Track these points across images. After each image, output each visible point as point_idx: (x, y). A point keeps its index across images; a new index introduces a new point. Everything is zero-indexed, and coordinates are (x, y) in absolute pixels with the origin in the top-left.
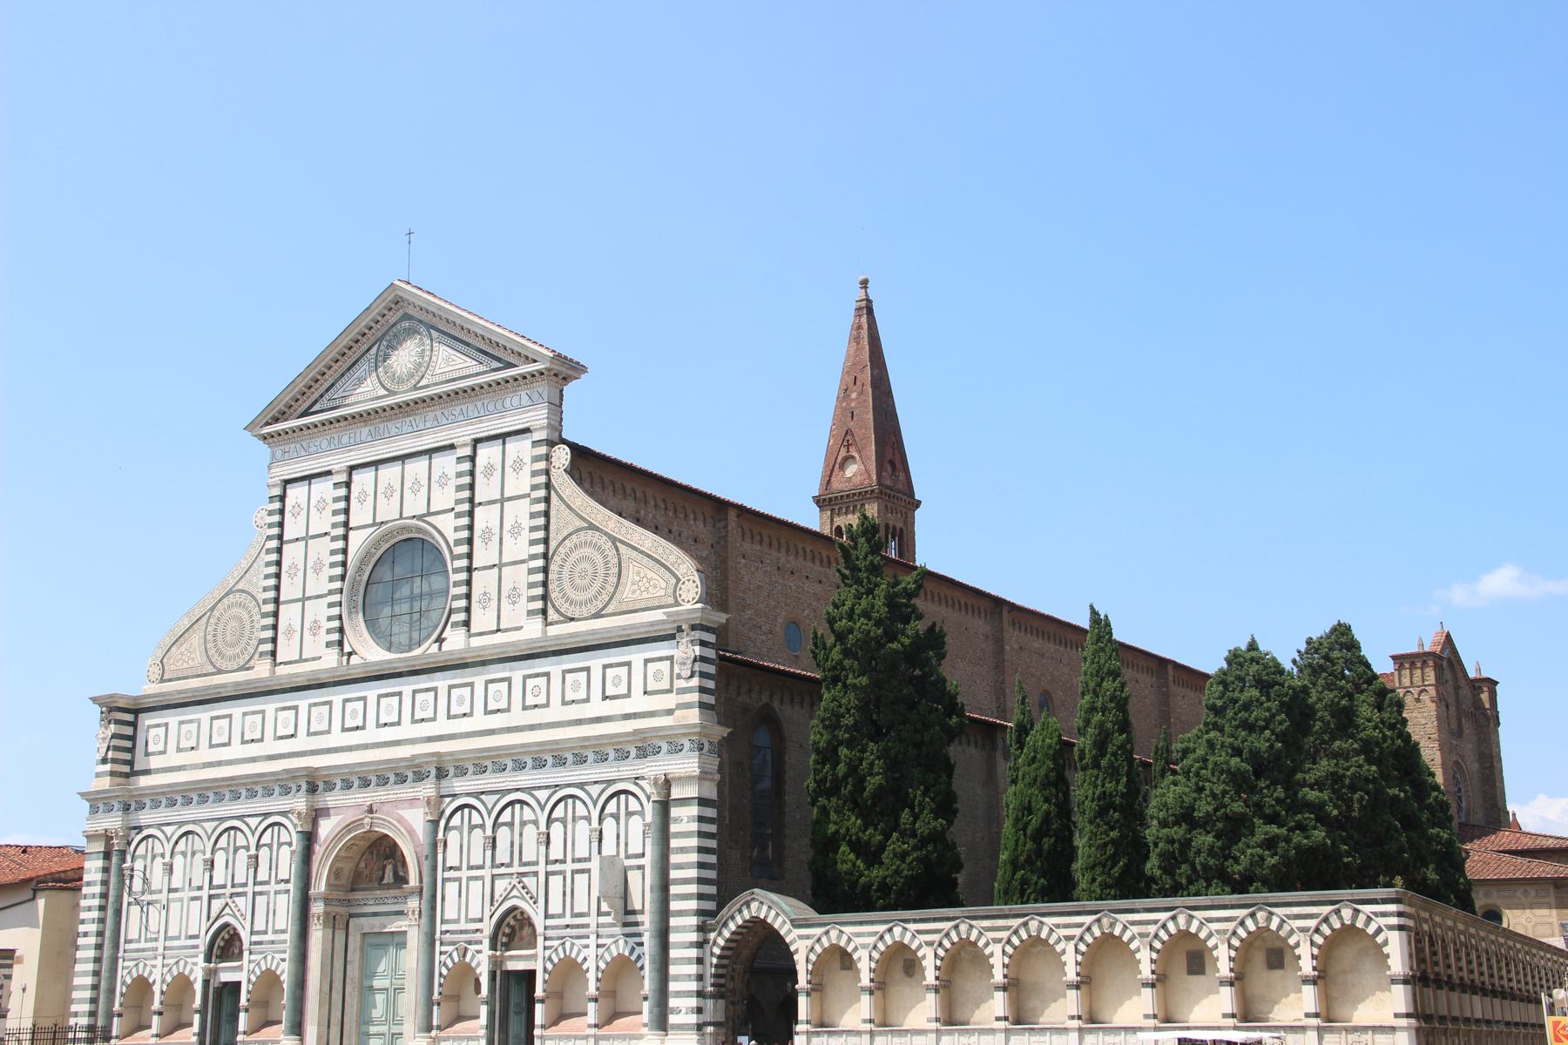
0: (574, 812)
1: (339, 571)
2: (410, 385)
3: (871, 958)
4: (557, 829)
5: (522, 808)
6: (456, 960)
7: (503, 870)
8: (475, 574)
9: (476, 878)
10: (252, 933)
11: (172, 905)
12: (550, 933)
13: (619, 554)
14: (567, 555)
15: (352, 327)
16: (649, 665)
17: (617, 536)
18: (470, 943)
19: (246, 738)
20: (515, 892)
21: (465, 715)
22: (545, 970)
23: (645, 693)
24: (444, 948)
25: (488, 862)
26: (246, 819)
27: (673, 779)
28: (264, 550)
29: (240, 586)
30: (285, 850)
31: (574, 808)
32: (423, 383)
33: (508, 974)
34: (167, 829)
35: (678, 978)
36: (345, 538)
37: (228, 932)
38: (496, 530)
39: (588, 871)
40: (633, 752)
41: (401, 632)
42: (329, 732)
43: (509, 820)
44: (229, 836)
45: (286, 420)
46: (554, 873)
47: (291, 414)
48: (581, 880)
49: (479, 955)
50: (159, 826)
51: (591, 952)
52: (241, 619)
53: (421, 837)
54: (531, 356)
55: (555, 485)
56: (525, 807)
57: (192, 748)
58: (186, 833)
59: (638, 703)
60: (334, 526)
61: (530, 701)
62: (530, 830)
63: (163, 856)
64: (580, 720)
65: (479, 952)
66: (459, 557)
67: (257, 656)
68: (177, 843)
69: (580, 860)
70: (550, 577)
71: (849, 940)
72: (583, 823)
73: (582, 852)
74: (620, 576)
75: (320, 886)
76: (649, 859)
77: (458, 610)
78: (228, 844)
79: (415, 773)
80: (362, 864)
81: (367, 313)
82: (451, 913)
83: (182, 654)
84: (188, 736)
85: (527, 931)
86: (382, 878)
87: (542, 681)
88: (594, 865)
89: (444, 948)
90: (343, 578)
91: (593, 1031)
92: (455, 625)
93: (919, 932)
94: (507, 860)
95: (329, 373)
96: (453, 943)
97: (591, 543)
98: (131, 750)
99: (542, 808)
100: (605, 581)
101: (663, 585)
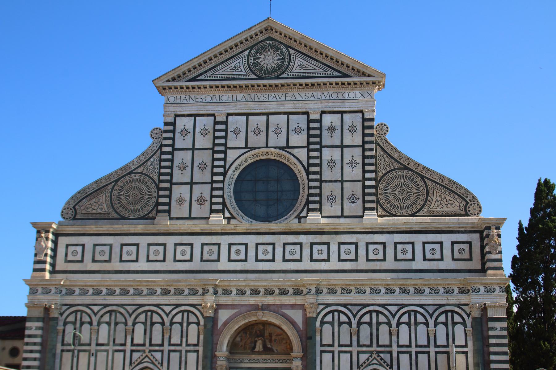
1: (221, 170)
2: (273, 76)
4: (404, 329)
5: (377, 315)
7: (364, 349)
8: (324, 184)
9: (346, 352)
11: (99, 354)
13: (426, 185)
15: (237, 37)
16: (455, 245)
19: (151, 258)
23: (453, 259)
25: (355, 343)
26: (161, 307)
27: (491, 306)
28: (159, 152)
29: (140, 170)
32: (284, 75)
34: (96, 309)
36: (225, 152)
40: (456, 291)
41: (261, 210)
43: (369, 321)
44: (146, 315)
45: (179, 81)
47: (184, 78)
50: (87, 306)
52: (140, 190)
54: (368, 72)
55: (380, 143)
56: (380, 314)
57: (105, 261)
58: (110, 312)
59: (448, 264)
61: (371, 256)
62: (384, 329)
63: (91, 323)
64: (409, 270)
67: (154, 212)
68: (102, 316)
70: (379, 191)
72: (424, 327)
75: (223, 349)
76: (472, 348)
79: (294, 290)
80: (238, 339)
81: (248, 31)
87: (380, 247)
88: (432, 350)
90: (224, 174)
92: (309, 210)
94: (368, 343)
95: (214, 59)
97: (406, 177)
98: (54, 257)
100: (418, 198)
101: (458, 204)
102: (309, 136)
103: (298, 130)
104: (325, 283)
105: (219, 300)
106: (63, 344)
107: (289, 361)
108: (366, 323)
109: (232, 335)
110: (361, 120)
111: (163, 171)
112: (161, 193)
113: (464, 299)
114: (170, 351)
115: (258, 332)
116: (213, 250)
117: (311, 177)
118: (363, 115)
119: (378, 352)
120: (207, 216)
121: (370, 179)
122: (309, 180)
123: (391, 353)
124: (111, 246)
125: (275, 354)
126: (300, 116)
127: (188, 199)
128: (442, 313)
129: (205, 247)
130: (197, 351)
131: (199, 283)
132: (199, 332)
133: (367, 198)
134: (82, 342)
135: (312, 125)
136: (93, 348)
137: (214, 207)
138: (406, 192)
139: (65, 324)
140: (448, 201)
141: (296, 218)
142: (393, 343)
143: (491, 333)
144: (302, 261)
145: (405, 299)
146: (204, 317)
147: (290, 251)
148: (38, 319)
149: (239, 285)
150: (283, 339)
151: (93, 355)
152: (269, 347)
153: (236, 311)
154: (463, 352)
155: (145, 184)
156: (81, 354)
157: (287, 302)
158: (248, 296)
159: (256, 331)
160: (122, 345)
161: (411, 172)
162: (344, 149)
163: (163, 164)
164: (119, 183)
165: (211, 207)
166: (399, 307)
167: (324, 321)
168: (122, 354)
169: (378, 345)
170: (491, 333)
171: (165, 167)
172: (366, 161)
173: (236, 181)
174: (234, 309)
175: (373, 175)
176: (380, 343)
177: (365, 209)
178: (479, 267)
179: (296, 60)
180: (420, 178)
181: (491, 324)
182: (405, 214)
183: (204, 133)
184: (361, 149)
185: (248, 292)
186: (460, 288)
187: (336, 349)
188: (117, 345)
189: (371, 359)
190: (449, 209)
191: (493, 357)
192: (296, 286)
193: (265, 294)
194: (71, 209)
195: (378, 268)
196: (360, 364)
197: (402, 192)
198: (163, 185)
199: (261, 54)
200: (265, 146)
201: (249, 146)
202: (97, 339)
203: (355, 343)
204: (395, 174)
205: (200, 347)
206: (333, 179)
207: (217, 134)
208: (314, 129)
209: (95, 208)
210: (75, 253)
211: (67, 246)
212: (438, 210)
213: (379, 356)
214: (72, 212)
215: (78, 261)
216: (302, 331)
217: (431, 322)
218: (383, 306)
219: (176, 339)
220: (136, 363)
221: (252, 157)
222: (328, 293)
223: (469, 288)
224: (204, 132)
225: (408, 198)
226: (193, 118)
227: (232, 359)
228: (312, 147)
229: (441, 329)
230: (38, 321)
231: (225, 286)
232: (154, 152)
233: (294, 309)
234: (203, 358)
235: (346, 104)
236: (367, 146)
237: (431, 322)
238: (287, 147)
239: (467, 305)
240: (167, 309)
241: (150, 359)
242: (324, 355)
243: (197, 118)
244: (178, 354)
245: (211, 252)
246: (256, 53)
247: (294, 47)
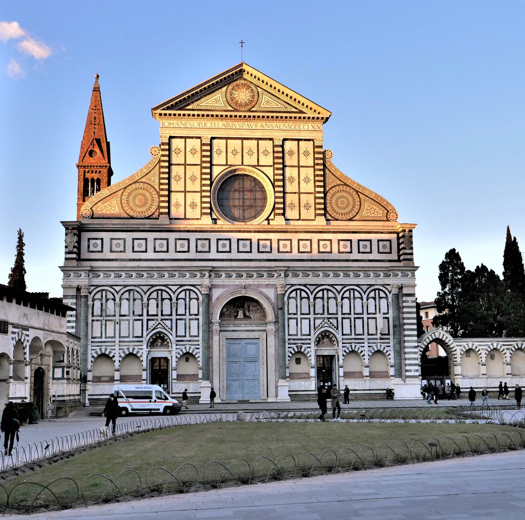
0: (354, 295)
3: (486, 354)
4: (346, 301)
5: (327, 292)
6: (296, 350)
7: (319, 316)
9: (306, 318)
10: (177, 336)
11: (122, 322)
12: (345, 341)
13: (360, 198)
14: (334, 194)
16: (380, 242)
17: (358, 190)
18: (304, 344)
20: (326, 325)
21: (287, 252)
22: (343, 355)
23: (379, 252)
24: (290, 346)
25: (312, 312)
26: (169, 287)
28: (158, 165)
29: (143, 180)
30: (194, 303)
31: (354, 294)
32: (254, 109)
33: (317, 356)
34: (118, 288)
35: (409, 359)
36: (211, 168)
37: (156, 336)
38: (297, 178)
39: (363, 318)
42: (209, 252)
43: (321, 296)
44: (158, 293)
46: (345, 318)
47: (176, 107)
48: (359, 322)
49: (309, 349)
50: (111, 286)
51: (366, 348)
52: (144, 196)
56: (329, 292)
57: (121, 252)
58: (129, 291)
59: (375, 255)
60: (202, 162)
62: (332, 302)
63: (114, 300)
64: (348, 260)
65: (310, 347)
66: (279, 186)
68: (122, 294)
69: (358, 314)
71: (476, 347)
72: (360, 300)
73: (359, 310)
74: (360, 207)
75: (216, 317)
77: (279, 209)
78: (158, 296)
80: (225, 310)
82: (293, 331)
83: (105, 206)
84: (118, 245)
85: (326, 340)
86: (237, 316)
87: (328, 243)
88: (365, 316)
89: (290, 346)
90: (211, 185)
91: (369, 378)
93: (504, 345)
94: (321, 312)
96: (295, 344)
98: (79, 248)
99: (339, 293)
100: (354, 207)
101: (382, 212)
102: (274, 158)
103: (266, 153)
106: (93, 316)
108: (319, 298)
110: (312, 147)
111: (162, 181)
112: (162, 199)
113: (387, 281)
114: (177, 319)
116: (205, 244)
117: (277, 189)
118: (314, 143)
119: (329, 318)
120: (199, 217)
121: (319, 192)
122: (275, 192)
123: (337, 318)
124: (125, 240)
126: (268, 141)
127: (183, 204)
128: (372, 291)
129: (199, 241)
130: (198, 319)
132: (198, 305)
133: (318, 206)
134: (108, 314)
135: (276, 149)
136: (117, 318)
137: (204, 211)
138: (346, 202)
139: (93, 300)
140: (375, 210)
141: (266, 220)
142: (339, 312)
143: (405, 304)
145: (347, 281)
146: (202, 294)
148: (72, 297)
151: (117, 324)
153: (226, 289)
154: (386, 318)
155: (149, 191)
156: (108, 322)
157: (263, 283)
158: (234, 279)
159: (238, 304)
160: (139, 315)
161: (349, 188)
162: (301, 168)
163: (162, 176)
164: (127, 190)
165: (201, 211)
166: (343, 286)
168: (140, 322)
169: (329, 314)
170: (405, 304)
171: (163, 178)
172: (317, 178)
173: (219, 190)
175: (322, 189)
176: (330, 312)
177: (316, 215)
178: (396, 258)
179: (263, 97)
180: (355, 193)
181: (405, 298)
182: (344, 219)
183: (193, 152)
184: (313, 169)
185: (234, 276)
186: (384, 274)
187: (299, 316)
188: (136, 316)
189: (323, 323)
190: (375, 215)
191: (406, 321)
193: (247, 277)
194: (89, 210)
195: (327, 259)
196: (316, 327)
197: (342, 203)
198: (162, 193)
199: (236, 90)
200: (241, 164)
201: (228, 164)
202: (120, 311)
203: (312, 312)
204: (338, 189)
206: (293, 192)
207: (204, 153)
208: (278, 152)
209: (109, 210)
210: (95, 245)
211: (89, 239)
212: (368, 216)
213: (329, 321)
214: (90, 212)
215: (98, 252)
217: (365, 297)
218: (332, 285)
219: (181, 311)
220: (152, 329)
221: (231, 172)
222: (293, 276)
223: (391, 274)
224: (193, 151)
225: (347, 207)
226: (184, 140)
228: (276, 166)
229: (371, 301)
230: (72, 299)
232: (154, 166)
235: (302, 134)
236: (317, 167)
237: (365, 297)
238: (257, 166)
239: (389, 285)
240: (174, 288)
241: (162, 326)
243: (187, 140)
244: (183, 321)
245: (203, 245)
246: (232, 89)
247: (261, 87)
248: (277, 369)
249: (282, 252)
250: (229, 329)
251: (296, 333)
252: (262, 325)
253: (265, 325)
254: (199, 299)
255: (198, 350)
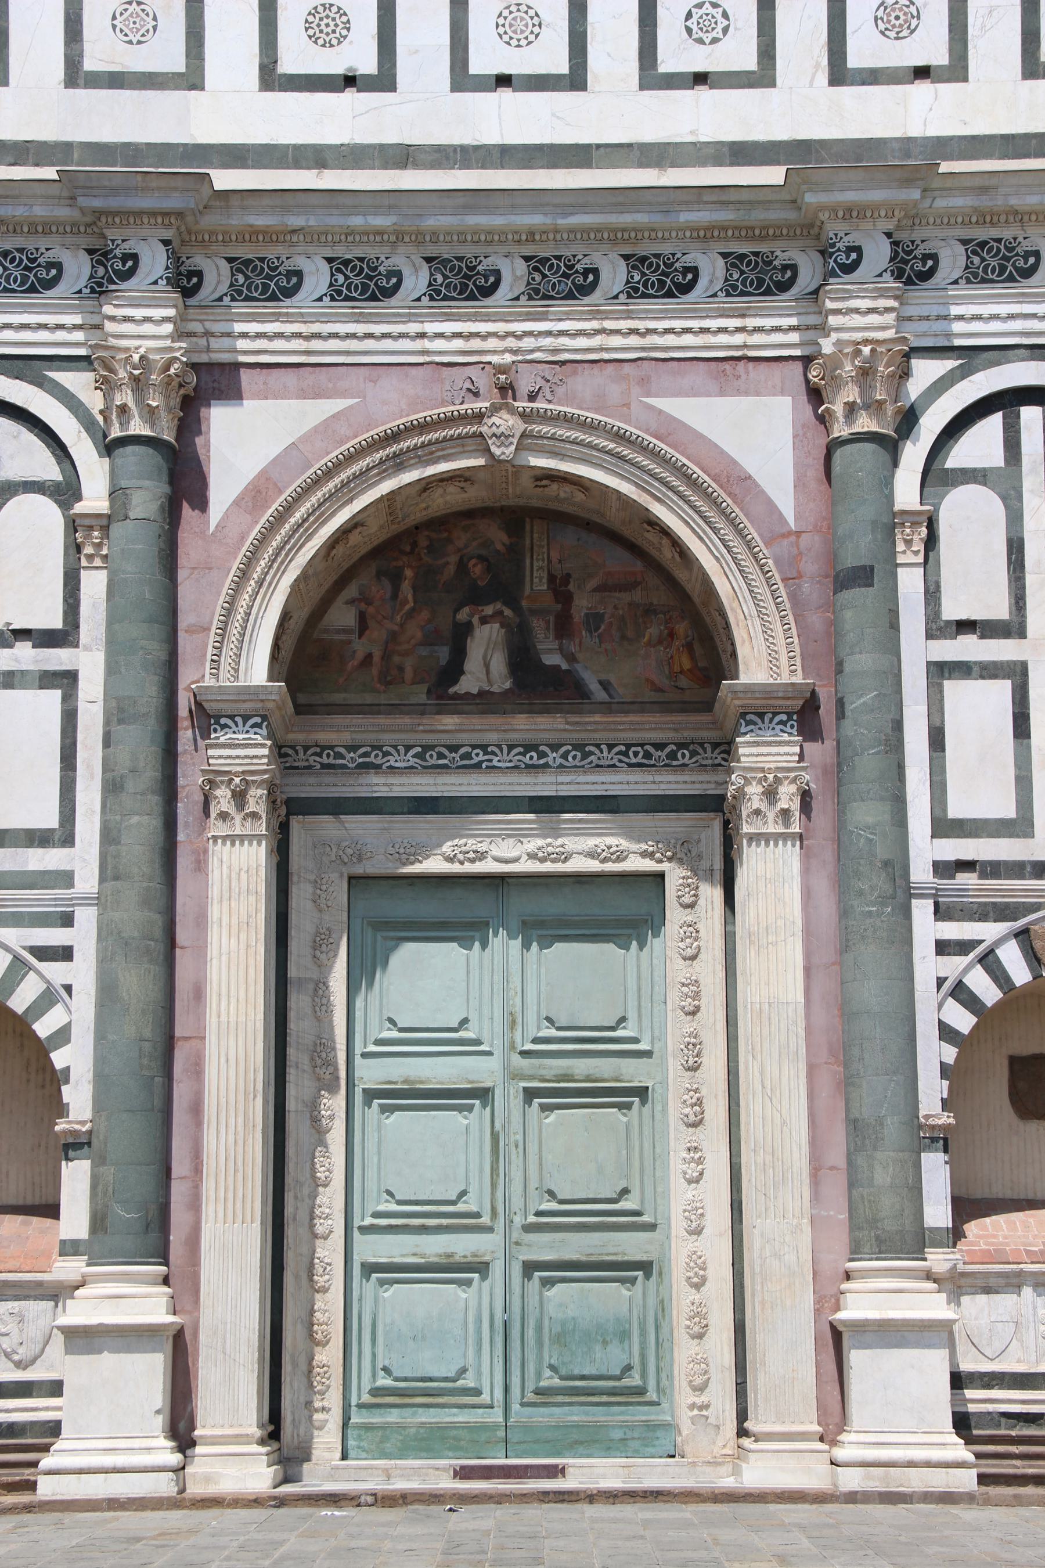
6: (1020, 974)
21: (922, 73)
24: (953, 931)
53: (786, 503)
79: (733, 260)
86: (454, 670)
89: (953, 931)
104: (960, 202)
105: (208, 334)
107: (693, 754)
109: (303, 577)
115: (477, 570)
125: (592, 712)
131: (63, 212)
132: (73, 549)
144: (772, 84)
147: (689, 15)
149: (350, 232)
150: (649, 611)
152: (556, 668)
159: (462, 566)
167: (951, 463)
174: (318, 395)
192: (747, 233)
205: (87, 649)
216: (798, 534)
222: (974, 276)
227: (306, 748)
231: (254, 234)
233: (739, 393)
234: (107, 723)
242: (953, 689)
248: (837, 1155)
249: (873, 77)
250: (382, 792)
251: (1008, 810)
252: (684, 757)
253: (709, 756)
254: (77, 495)
255: (56, 971)
